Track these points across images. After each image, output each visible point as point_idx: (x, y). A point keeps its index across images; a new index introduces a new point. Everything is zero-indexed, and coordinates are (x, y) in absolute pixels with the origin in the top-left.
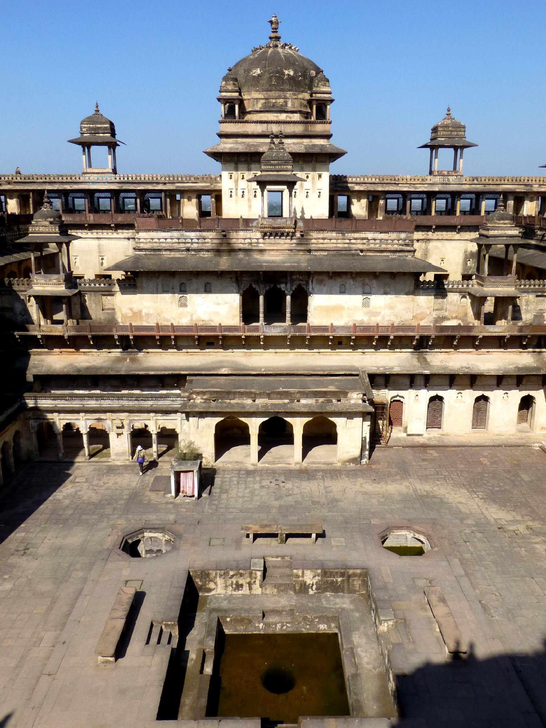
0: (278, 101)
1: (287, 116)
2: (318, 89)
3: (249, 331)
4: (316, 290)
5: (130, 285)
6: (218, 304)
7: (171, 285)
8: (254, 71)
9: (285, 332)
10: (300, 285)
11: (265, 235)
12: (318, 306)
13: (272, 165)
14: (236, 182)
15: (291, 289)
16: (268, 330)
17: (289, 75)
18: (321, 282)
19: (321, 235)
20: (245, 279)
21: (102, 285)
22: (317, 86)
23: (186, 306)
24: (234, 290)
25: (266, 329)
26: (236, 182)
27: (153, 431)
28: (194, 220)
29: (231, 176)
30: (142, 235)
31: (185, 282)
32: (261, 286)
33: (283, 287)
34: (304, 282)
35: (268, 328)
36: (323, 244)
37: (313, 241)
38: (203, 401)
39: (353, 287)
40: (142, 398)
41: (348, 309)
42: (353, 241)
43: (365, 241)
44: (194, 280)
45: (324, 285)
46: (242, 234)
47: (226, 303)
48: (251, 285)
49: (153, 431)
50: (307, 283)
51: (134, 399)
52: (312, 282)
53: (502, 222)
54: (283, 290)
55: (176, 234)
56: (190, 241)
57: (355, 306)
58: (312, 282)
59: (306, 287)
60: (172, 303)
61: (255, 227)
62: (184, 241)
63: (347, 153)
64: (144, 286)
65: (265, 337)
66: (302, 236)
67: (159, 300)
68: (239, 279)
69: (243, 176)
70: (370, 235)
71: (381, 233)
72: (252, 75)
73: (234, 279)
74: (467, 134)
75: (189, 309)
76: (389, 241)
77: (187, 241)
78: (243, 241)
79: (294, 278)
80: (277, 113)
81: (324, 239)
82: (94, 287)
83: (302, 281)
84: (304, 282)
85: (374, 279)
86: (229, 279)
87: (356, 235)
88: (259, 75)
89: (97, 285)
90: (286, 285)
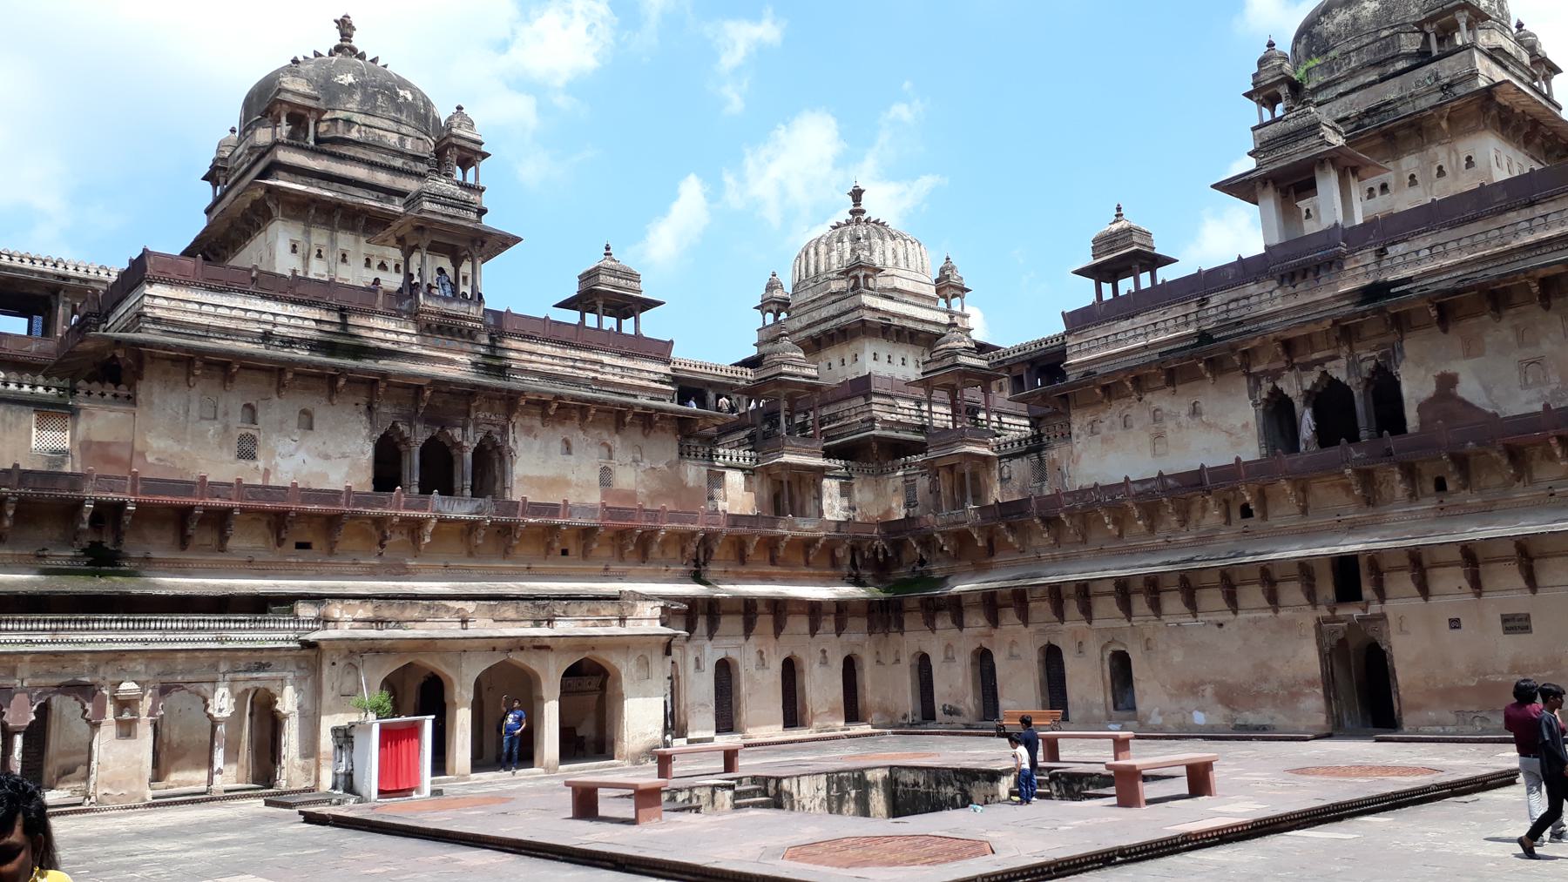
0: (389, 135)
1: (404, 163)
2: (460, 132)
3: (407, 507)
4: (520, 443)
5: (115, 396)
6: (327, 457)
7: (221, 405)
8: (341, 77)
9: (477, 513)
10: (489, 432)
11: (428, 326)
12: (525, 477)
13: (444, 204)
14: (306, 260)
15: (475, 438)
16: (446, 505)
17: (406, 99)
18: (529, 431)
19: (525, 346)
20: (384, 410)
21: (40, 390)
22: (459, 127)
23: (254, 457)
24: (362, 430)
25: (443, 502)
26: (306, 260)
27: (220, 710)
28: (284, 276)
29: (294, 246)
30: (157, 289)
31: (254, 403)
32: (419, 427)
33: (457, 433)
34: (498, 429)
35: (447, 503)
36: (531, 362)
37: (512, 354)
38: (357, 625)
39: (585, 444)
40: (201, 625)
41: (577, 485)
42: (579, 364)
43: (597, 367)
44: (275, 398)
45: (535, 436)
46: (378, 322)
47: (344, 456)
48: (394, 422)
49: (220, 710)
50: (505, 430)
51: (180, 625)
52: (514, 427)
53: (794, 354)
54: (459, 439)
55: (238, 301)
56: (271, 318)
57: (588, 481)
58: (514, 427)
59: (501, 438)
60: (220, 447)
61: (406, 312)
62: (256, 316)
63: (520, 240)
64: (156, 401)
65: (441, 521)
66: (491, 339)
67: (189, 437)
68: (376, 406)
69: (319, 251)
70: (606, 359)
71: (623, 355)
72: (336, 83)
73: (363, 408)
74: (642, 286)
75: (261, 464)
76: (636, 373)
77: (264, 317)
78: (381, 335)
79: (481, 416)
80: (387, 154)
81: (531, 353)
82: (14, 392)
83: (494, 425)
84: (498, 429)
85: (617, 432)
86: (353, 406)
87: (584, 355)
88: (350, 84)
89: (26, 388)
90: (465, 428)
